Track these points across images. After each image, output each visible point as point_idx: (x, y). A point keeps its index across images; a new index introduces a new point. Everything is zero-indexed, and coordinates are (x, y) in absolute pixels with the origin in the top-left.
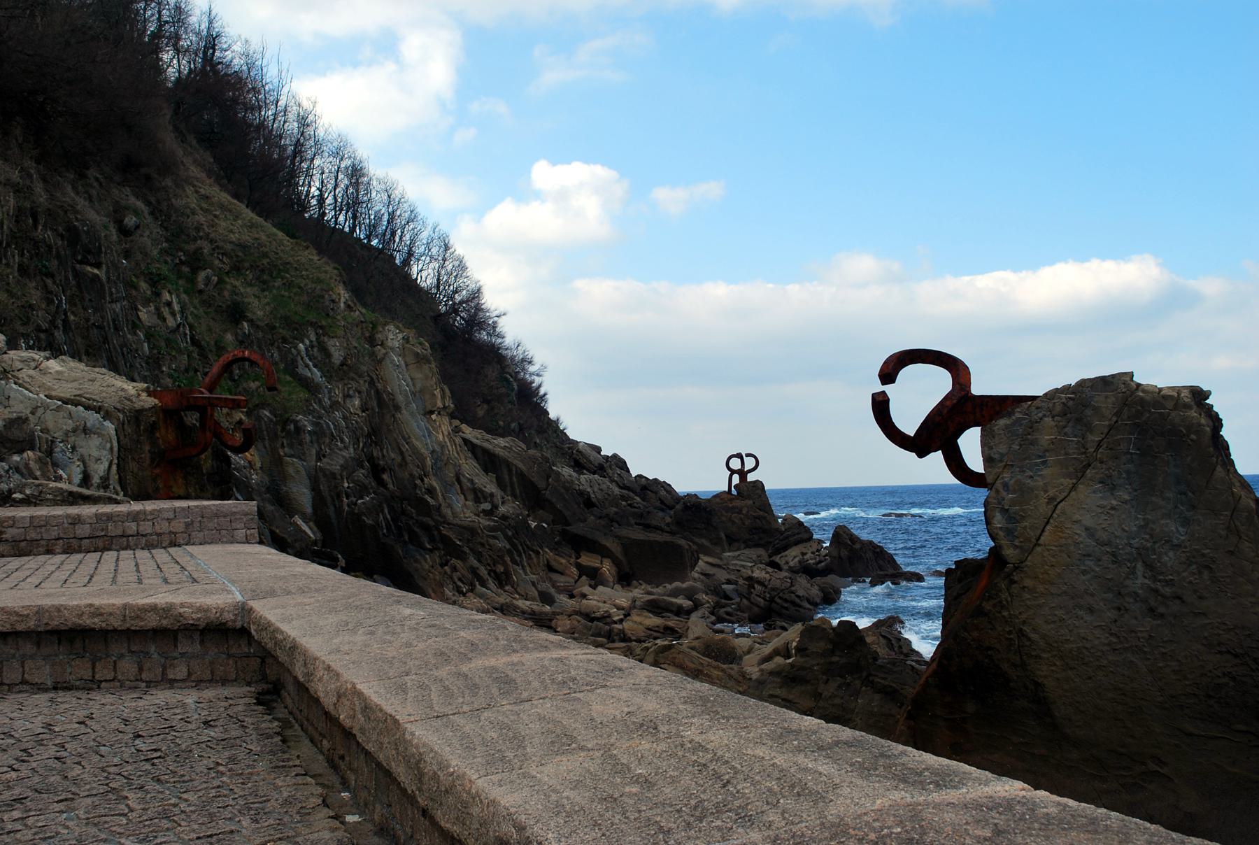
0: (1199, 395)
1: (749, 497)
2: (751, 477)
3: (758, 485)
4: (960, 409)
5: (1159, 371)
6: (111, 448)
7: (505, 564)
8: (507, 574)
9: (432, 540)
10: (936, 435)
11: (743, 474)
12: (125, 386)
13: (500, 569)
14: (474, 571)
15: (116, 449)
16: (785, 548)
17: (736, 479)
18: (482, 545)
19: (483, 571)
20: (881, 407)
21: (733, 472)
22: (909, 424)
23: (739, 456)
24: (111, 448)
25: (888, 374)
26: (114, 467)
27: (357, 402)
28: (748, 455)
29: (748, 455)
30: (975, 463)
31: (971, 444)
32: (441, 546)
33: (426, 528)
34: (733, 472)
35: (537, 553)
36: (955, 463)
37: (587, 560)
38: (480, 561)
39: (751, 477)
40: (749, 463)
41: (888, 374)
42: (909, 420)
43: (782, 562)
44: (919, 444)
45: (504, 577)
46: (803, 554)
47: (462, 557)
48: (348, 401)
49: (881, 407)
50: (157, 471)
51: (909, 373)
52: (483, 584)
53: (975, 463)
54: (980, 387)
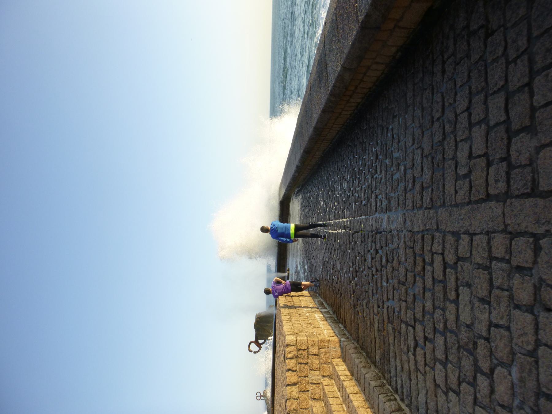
0: (256, 315)
2: (262, 394)
4: (256, 342)
5: (253, 320)
10: (259, 345)
11: (261, 396)
17: (262, 398)
20: (255, 352)
21: (260, 399)
22: (258, 349)
23: (257, 397)
25: (251, 351)
30: (263, 341)
31: (260, 342)
36: (263, 343)
39: (262, 394)
40: (259, 394)
41: (251, 351)
42: (258, 349)
44: (260, 348)
49: (255, 352)
51: (251, 348)
53: (263, 341)
54: (254, 340)
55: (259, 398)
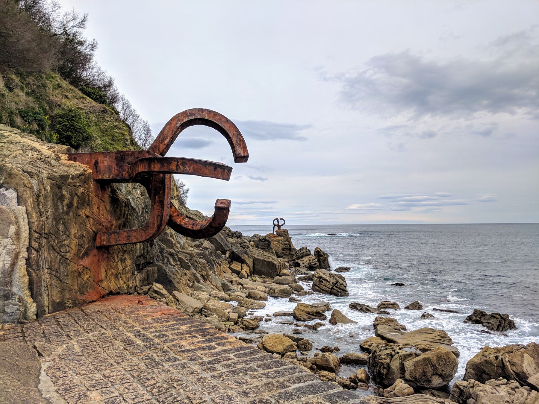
1: (281, 236)
3: (286, 232)
6: (18, 233)
7: (206, 270)
8: (208, 275)
9: (174, 260)
11: (279, 227)
12: (37, 146)
13: (204, 273)
14: (194, 275)
15: (25, 234)
16: (302, 257)
18: (196, 261)
19: (198, 275)
21: (275, 225)
23: (277, 219)
24: (18, 233)
26: (22, 263)
27: (139, 191)
28: (281, 219)
29: (281, 219)
32: (179, 263)
33: (171, 255)
34: (275, 225)
35: (220, 265)
37: (236, 266)
38: (196, 270)
39: (282, 228)
40: (281, 222)
43: (301, 263)
45: (206, 277)
46: (310, 260)
47: (188, 268)
48: (134, 190)
50: (86, 262)
52: (198, 282)
55: (276, 223)
